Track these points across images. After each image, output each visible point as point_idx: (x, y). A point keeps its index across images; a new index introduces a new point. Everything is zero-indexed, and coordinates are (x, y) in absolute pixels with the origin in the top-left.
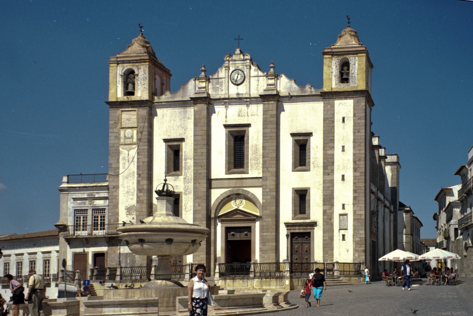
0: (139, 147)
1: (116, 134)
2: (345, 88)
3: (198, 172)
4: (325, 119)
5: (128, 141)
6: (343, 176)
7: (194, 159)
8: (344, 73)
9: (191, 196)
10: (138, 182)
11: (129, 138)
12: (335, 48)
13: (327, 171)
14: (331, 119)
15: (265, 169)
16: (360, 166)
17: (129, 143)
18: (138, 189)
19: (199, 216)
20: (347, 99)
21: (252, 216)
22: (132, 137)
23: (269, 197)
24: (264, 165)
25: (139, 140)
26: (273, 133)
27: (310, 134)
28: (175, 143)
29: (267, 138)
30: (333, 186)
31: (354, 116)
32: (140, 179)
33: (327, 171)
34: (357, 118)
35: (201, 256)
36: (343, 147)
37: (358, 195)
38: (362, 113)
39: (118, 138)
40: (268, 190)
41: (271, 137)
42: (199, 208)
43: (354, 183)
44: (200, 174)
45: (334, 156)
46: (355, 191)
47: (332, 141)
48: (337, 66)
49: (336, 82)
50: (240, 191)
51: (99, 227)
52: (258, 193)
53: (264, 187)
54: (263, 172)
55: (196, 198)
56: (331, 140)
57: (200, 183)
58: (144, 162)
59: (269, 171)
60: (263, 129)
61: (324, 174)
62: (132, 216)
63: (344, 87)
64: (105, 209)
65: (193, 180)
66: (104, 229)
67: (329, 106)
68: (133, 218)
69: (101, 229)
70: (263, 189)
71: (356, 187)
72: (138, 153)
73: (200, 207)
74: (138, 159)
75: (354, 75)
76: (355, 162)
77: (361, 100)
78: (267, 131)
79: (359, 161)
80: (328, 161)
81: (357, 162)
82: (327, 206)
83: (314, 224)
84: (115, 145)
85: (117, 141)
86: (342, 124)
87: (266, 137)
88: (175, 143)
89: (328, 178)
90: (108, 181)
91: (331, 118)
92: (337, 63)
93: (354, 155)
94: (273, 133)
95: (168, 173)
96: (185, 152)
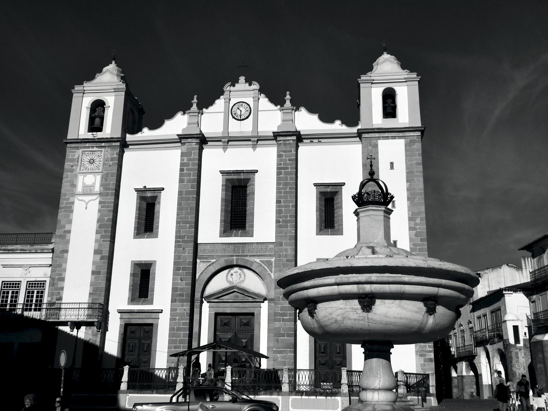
8: (387, 106)
20: (396, 139)
21: (256, 297)
39: (74, 186)
50: (240, 262)
51: (33, 307)
63: (390, 123)
64: (45, 281)
66: (40, 310)
69: (35, 310)
88: (149, 194)
90: (54, 243)
95: (137, 235)
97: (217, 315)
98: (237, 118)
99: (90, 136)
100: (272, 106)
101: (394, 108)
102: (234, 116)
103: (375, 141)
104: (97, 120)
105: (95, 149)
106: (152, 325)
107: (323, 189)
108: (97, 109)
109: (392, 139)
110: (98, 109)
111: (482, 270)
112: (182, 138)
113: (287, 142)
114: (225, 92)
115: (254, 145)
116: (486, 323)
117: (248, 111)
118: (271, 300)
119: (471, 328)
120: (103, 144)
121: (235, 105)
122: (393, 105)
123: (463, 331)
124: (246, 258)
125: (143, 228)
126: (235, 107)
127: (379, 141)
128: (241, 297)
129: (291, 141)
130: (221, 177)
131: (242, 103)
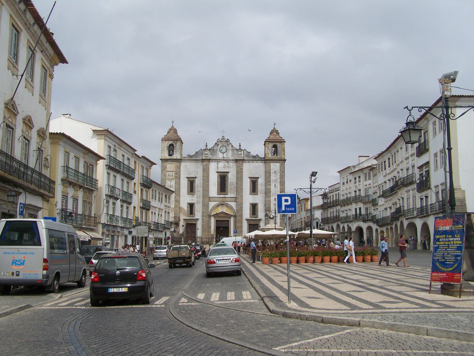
1: (164, 174)
2: (276, 158)
3: (205, 194)
4: (266, 172)
5: (170, 178)
7: (203, 188)
9: (201, 205)
10: (175, 197)
11: (170, 176)
12: (270, 139)
13: (267, 196)
15: (238, 194)
17: (171, 178)
18: (175, 201)
19: (205, 214)
22: (172, 176)
23: (239, 207)
25: (176, 177)
28: (192, 179)
30: (270, 203)
31: (280, 171)
32: (176, 196)
33: (267, 196)
34: (281, 172)
35: (206, 234)
36: (275, 185)
40: (239, 204)
42: (206, 211)
44: (206, 194)
52: (233, 204)
53: (237, 202)
55: (204, 206)
56: (269, 181)
57: (206, 199)
58: (178, 188)
60: (237, 175)
61: (266, 197)
62: (172, 213)
63: (275, 157)
65: (201, 198)
67: (268, 166)
68: (173, 214)
72: (175, 183)
74: (175, 186)
78: (239, 176)
83: (260, 220)
84: (164, 179)
85: (165, 177)
88: (192, 179)
89: (267, 199)
93: (280, 189)
97: (217, 221)
99: (169, 157)
101: (277, 151)
103: (269, 164)
104: (171, 151)
105: (172, 163)
107: (252, 179)
112: (203, 160)
125: (190, 191)
127: (271, 164)
128: (224, 215)
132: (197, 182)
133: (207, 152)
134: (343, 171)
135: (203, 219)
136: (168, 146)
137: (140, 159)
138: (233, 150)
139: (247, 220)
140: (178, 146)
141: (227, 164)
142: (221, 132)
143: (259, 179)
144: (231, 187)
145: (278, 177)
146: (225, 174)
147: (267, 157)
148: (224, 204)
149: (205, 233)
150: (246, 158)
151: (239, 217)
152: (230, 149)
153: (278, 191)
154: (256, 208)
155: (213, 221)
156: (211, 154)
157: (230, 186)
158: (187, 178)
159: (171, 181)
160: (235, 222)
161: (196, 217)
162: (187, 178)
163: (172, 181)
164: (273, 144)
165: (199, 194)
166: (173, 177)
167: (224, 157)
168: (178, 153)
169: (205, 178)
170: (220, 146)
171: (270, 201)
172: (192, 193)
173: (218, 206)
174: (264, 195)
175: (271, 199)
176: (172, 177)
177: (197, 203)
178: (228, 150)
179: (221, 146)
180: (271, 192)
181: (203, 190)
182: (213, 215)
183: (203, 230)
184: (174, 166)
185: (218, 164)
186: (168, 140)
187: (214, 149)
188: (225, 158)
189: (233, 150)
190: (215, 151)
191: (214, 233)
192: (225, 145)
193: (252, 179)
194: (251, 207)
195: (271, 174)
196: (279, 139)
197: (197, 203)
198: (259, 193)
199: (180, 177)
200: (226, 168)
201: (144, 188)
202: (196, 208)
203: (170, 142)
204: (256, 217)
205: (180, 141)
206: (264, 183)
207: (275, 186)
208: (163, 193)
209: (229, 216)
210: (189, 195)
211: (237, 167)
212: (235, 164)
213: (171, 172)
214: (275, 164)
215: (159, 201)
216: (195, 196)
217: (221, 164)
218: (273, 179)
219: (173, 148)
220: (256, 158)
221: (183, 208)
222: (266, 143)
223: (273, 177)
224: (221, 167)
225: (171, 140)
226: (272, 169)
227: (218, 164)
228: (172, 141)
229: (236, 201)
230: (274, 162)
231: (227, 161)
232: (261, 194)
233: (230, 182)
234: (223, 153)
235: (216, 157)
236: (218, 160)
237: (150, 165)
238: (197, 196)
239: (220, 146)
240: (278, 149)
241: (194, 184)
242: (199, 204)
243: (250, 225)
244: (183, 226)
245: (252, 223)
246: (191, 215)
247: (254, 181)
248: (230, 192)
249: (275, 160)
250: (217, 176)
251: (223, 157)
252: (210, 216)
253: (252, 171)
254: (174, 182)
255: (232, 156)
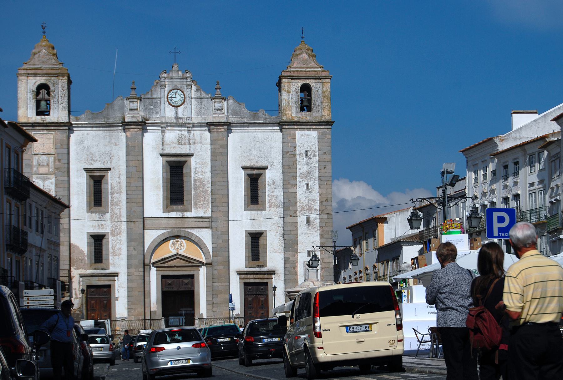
0: (58, 178)
4: (284, 153)
5: (43, 170)
6: (308, 218)
9: (124, 237)
11: (43, 166)
13: (289, 212)
14: (292, 153)
15: (215, 209)
16: (327, 207)
19: (135, 262)
20: (310, 131)
22: (48, 165)
24: (213, 204)
25: (57, 169)
26: (224, 166)
27: (265, 168)
29: (216, 172)
31: (319, 148)
33: (289, 212)
34: (322, 152)
36: (307, 185)
37: (326, 241)
38: (328, 146)
40: (219, 233)
41: (221, 170)
42: (134, 253)
43: (321, 227)
44: (135, 212)
45: (297, 195)
46: (322, 236)
47: (294, 177)
48: (297, 92)
49: (296, 110)
52: (206, 236)
53: (214, 229)
54: (212, 211)
55: (130, 240)
56: (293, 176)
59: (220, 211)
63: (305, 116)
67: (289, 138)
70: (212, 231)
71: (323, 231)
72: (56, 185)
73: (136, 252)
75: (317, 103)
76: (321, 202)
77: (326, 131)
79: (326, 201)
80: (290, 201)
81: (324, 203)
82: (290, 252)
86: (305, 158)
87: (215, 170)
89: (290, 220)
91: (292, 151)
92: (297, 89)
93: (320, 194)
94: (224, 166)
96: (111, 184)
97: (164, 277)
98: (173, 104)
99: (39, 119)
100: (204, 95)
101: (310, 101)
102: (170, 102)
104: (43, 103)
106: (109, 287)
107: (250, 172)
108: (41, 91)
109: (308, 130)
110: (42, 91)
111: (389, 213)
113: (219, 131)
114: (162, 80)
115: (189, 130)
116: (388, 269)
117: (182, 98)
118: (208, 265)
119: (376, 273)
120: (52, 128)
121: (170, 91)
122: (309, 98)
123: (368, 275)
124: (185, 230)
125: (93, 203)
126: (170, 93)
127: (297, 132)
128: (183, 263)
129: (223, 130)
130: (162, 160)
131: (177, 90)
132: (111, 180)
133: (136, 104)
134: (475, 149)
135: (129, 274)
136: (35, 89)
137: (6, 129)
138: (201, 98)
139: (239, 273)
140: (60, 89)
141: (186, 133)
142: (171, 52)
143: (267, 171)
144: (198, 191)
145: (313, 165)
146: (183, 159)
147: (286, 115)
148: (182, 234)
149: (135, 310)
150: (232, 119)
151: (221, 267)
152: (193, 96)
153: (314, 200)
154: (261, 242)
155: (154, 275)
156: (146, 109)
157: (195, 189)
158: (86, 170)
159: (44, 180)
160: (211, 279)
161: (111, 270)
162: (86, 170)
163: (48, 179)
164: (300, 83)
165: (116, 212)
166: (51, 170)
167: (180, 115)
168: (61, 106)
169: (133, 169)
170: (167, 89)
171: (295, 225)
172: (98, 209)
173: (166, 240)
174: (281, 210)
175: (299, 220)
176: (47, 168)
177: (112, 234)
178: (188, 100)
179: (171, 89)
180: (298, 204)
181: (129, 201)
182: (153, 264)
183: (131, 303)
184: (52, 141)
185: (163, 134)
186: (35, 75)
187: (154, 96)
188: (182, 119)
189: (201, 98)
190: (154, 101)
191: (157, 308)
192: (179, 86)
193: (250, 172)
194: (250, 239)
195: (298, 157)
196: (315, 71)
197: (113, 235)
198: (267, 205)
199: (69, 168)
200: (185, 144)
201: (13, 199)
202: (110, 247)
203: (38, 78)
204: (263, 266)
205: (66, 78)
206: (279, 181)
207: (307, 188)
208: (44, 210)
209: (196, 264)
210: (92, 213)
211: (213, 142)
212: (207, 135)
213: (45, 157)
214: (307, 132)
215: (37, 231)
216: (108, 215)
217: (171, 135)
218: (301, 171)
219: (49, 94)
220: (258, 120)
221: (78, 248)
222: (284, 80)
223: (302, 166)
224: (172, 142)
225: (43, 75)
226: (300, 146)
227: (163, 134)
228: (44, 78)
229: (211, 228)
230: (303, 127)
231: (189, 125)
232: (272, 209)
233: (195, 180)
234: (177, 107)
235: (158, 116)
236: (162, 123)
237: (23, 144)
238: (112, 216)
239: (167, 89)
240: (313, 95)
241: (103, 186)
242: (118, 237)
243: (246, 284)
244: (83, 291)
245: (252, 281)
246: (99, 265)
247: (254, 176)
248: (196, 205)
249: (307, 123)
250: (163, 166)
251: (177, 118)
252: (145, 266)
253: (250, 150)
254: (53, 180)
255: (199, 113)
